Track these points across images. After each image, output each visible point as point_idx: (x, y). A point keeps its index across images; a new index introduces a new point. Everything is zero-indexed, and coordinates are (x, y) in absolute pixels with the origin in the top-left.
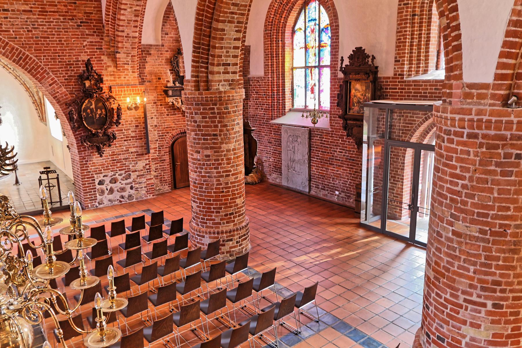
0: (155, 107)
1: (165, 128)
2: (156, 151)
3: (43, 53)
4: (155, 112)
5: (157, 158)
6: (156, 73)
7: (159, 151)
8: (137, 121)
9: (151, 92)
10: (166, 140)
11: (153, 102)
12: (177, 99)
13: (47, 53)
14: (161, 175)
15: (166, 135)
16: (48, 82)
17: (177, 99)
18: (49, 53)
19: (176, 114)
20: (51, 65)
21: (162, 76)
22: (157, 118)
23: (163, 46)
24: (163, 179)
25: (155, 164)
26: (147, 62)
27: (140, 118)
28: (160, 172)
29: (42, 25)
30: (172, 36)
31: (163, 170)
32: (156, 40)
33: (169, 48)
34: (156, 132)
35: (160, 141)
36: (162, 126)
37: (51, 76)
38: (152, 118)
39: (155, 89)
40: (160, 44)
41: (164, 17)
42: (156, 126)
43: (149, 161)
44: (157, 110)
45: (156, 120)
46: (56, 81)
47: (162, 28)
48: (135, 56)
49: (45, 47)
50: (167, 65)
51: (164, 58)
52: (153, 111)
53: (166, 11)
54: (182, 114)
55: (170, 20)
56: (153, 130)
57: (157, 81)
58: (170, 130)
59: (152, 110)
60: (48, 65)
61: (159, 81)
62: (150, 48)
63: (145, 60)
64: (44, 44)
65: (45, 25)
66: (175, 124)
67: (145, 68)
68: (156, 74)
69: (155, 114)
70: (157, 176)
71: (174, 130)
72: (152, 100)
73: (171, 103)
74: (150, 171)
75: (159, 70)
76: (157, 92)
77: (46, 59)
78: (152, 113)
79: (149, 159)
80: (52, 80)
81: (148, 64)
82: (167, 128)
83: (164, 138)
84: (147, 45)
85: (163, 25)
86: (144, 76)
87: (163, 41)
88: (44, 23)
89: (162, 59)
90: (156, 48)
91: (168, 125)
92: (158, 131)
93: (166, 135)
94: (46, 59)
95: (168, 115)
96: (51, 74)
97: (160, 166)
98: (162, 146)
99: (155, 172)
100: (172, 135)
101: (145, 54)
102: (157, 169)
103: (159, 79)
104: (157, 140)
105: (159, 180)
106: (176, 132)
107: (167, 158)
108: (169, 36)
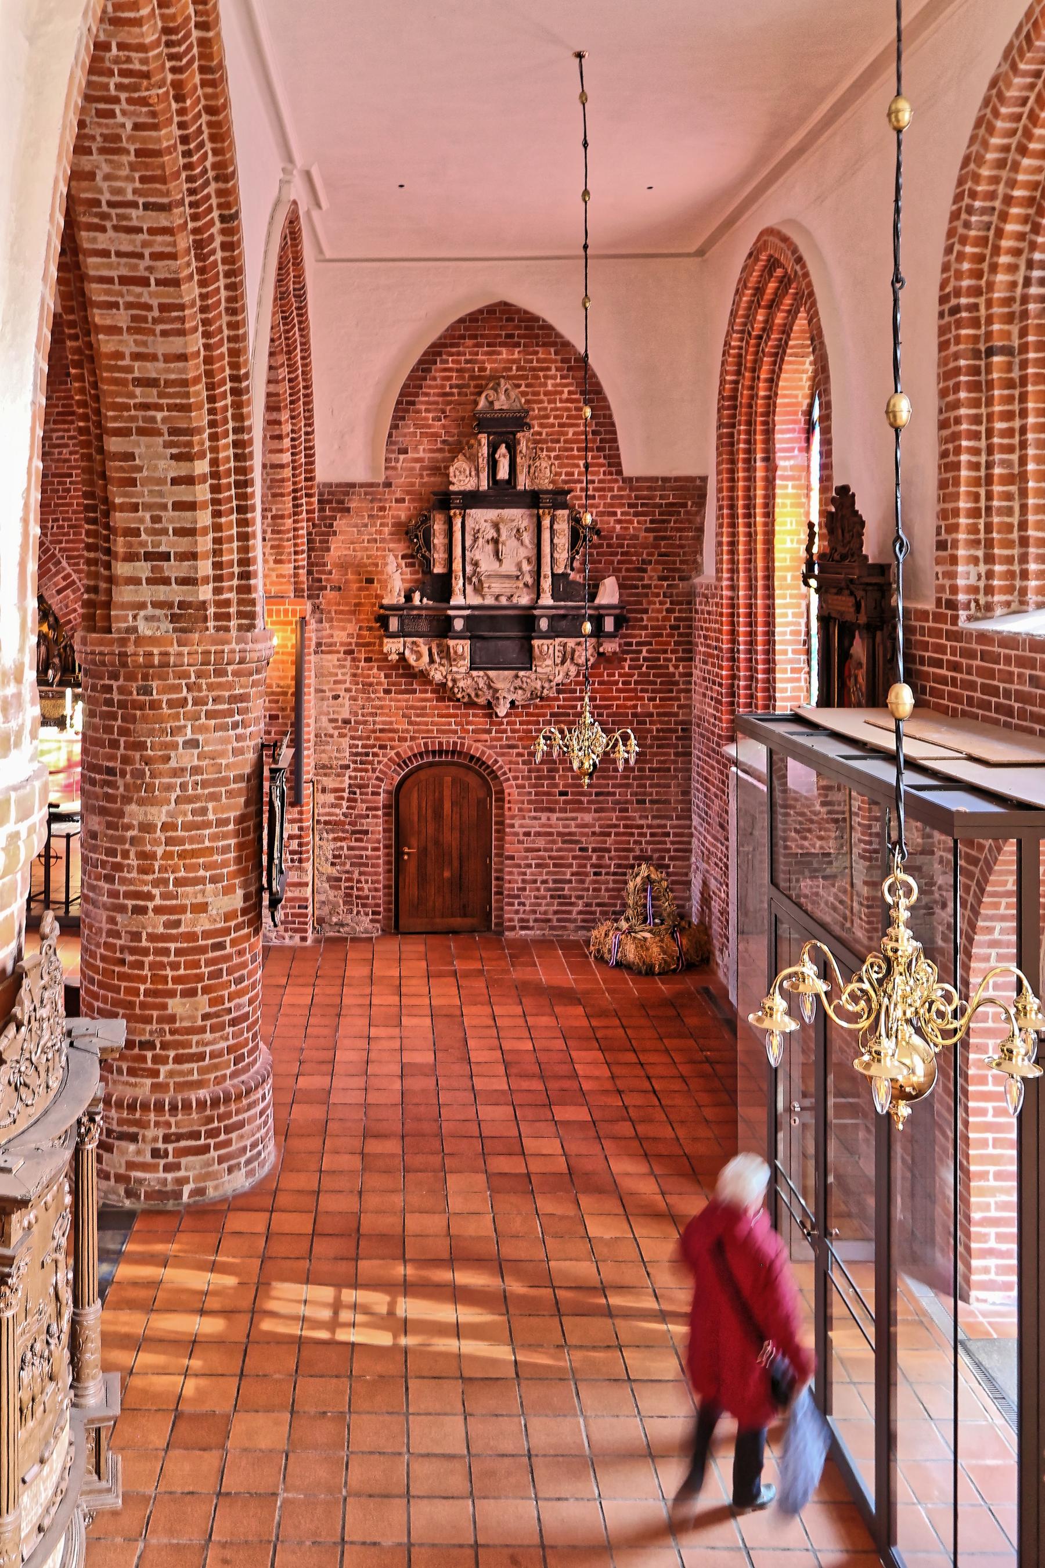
0: (348, 663)
1: (374, 731)
2: (342, 798)
3: (54, 512)
4: (348, 678)
5: (343, 823)
6: (358, 566)
7: (349, 800)
8: (277, 702)
9: (340, 620)
10: (374, 770)
11: (342, 649)
12: (414, 643)
13: (61, 512)
14: (348, 880)
15: (375, 755)
16: (56, 584)
17: (414, 643)
18: (67, 512)
19: (414, 692)
20: (67, 542)
21: (377, 573)
22: (353, 699)
23: (388, 485)
24: (355, 892)
25: (335, 839)
26: (335, 533)
27: (285, 694)
28: (348, 867)
29: (59, 446)
30: (421, 454)
31: (359, 862)
32: (374, 469)
33: (408, 493)
34: (345, 742)
35: (355, 770)
36: (365, 723)
37: (64, 569)
38: (336, 697)
39: (354, 613)
40: (381, 479)
41: (399, 402)
42: (346, 722)
43: (301, 829)
44: (354, 675)
45: (347, 703)
46: (73, 582)
47: (390, 435)
48: (282, 517)
49: (59, 498)
50: (399, 541)
51: (390, 521)
52: (340, 677)
53: (406, 386)
54: (433, 691)
55: (419, 411)
56: (336, 733)
57: (360, 589)
58: (392, 739)
59: (339, 672)
60: (61, 542)
61: (367, 589)
62: (347, 494)
63: (331, 526)
64: (58, 491)
65: (66, 446)
66: (410, 723)
67: (328, 549)
68: (359, 568)
69: (348, 685)
70: (339, 879)
71: (405, 740)
72: (342, 644)
73: (394, 657)
74: (300, 861)
75: (369, 557)
76: (358, 621)
77: (59, 527)
78: (336, 682)
79: (300, 821)
80: (64, 578)
81: (340, 537)
82: (382, 731)
83: (371, 763)
84: (338, 485)
85: (394, 426)
86: (323, 572)
87: (389, 472)
88: (66, 441)
89: (382, 525)
90: (366, 494)
91: (384, 723)
92: (353, 738)
93: (375, 755)
94: (59, 527)
95: (387, 692)
96: (64, 563)
97: (350, 848)
98: (360, 787)
99: (333, 864)
100: (398, 754)
101: (332, 509)
102: (339, 857)
103: (370, 581)
104: (347, 767)
105: (341, 893)
106: (411, 748)
107: (377, 826)
108: (410, 455)
